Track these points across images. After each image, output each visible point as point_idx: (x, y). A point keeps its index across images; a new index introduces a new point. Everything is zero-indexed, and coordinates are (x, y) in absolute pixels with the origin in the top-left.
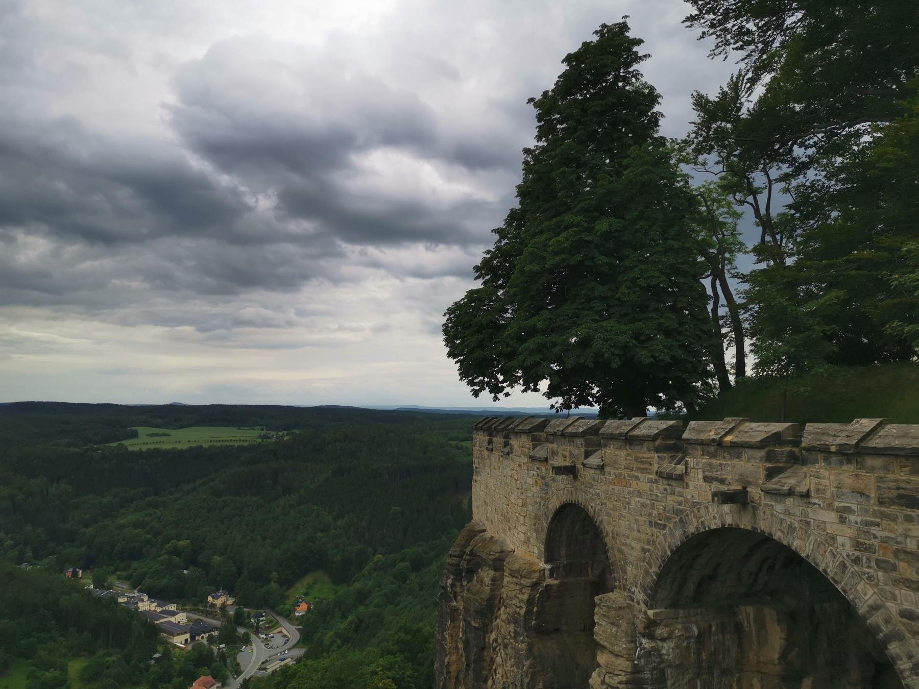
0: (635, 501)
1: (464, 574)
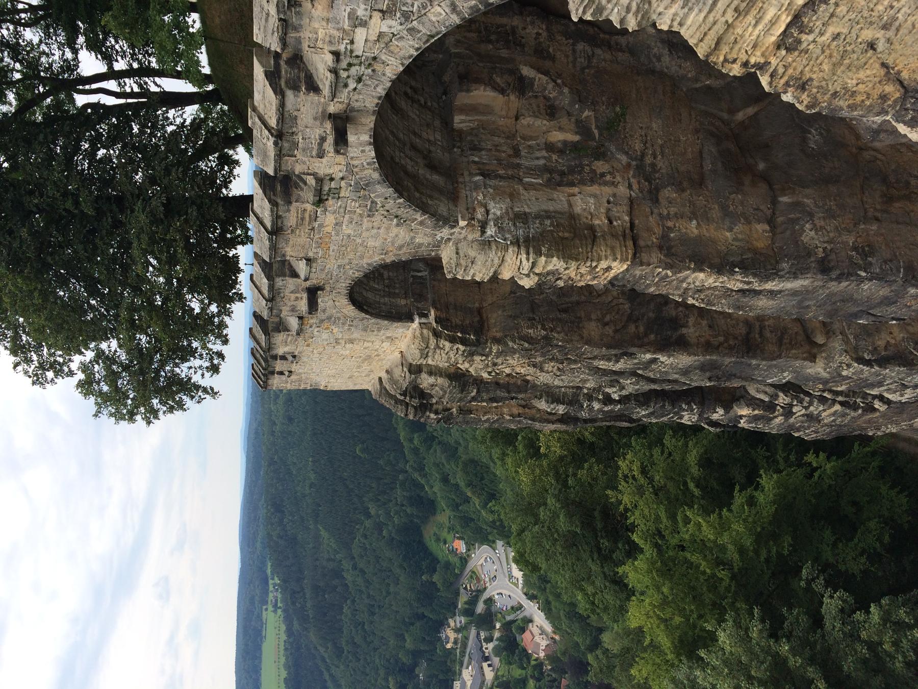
0: (347, 230)
1: (425, 402)
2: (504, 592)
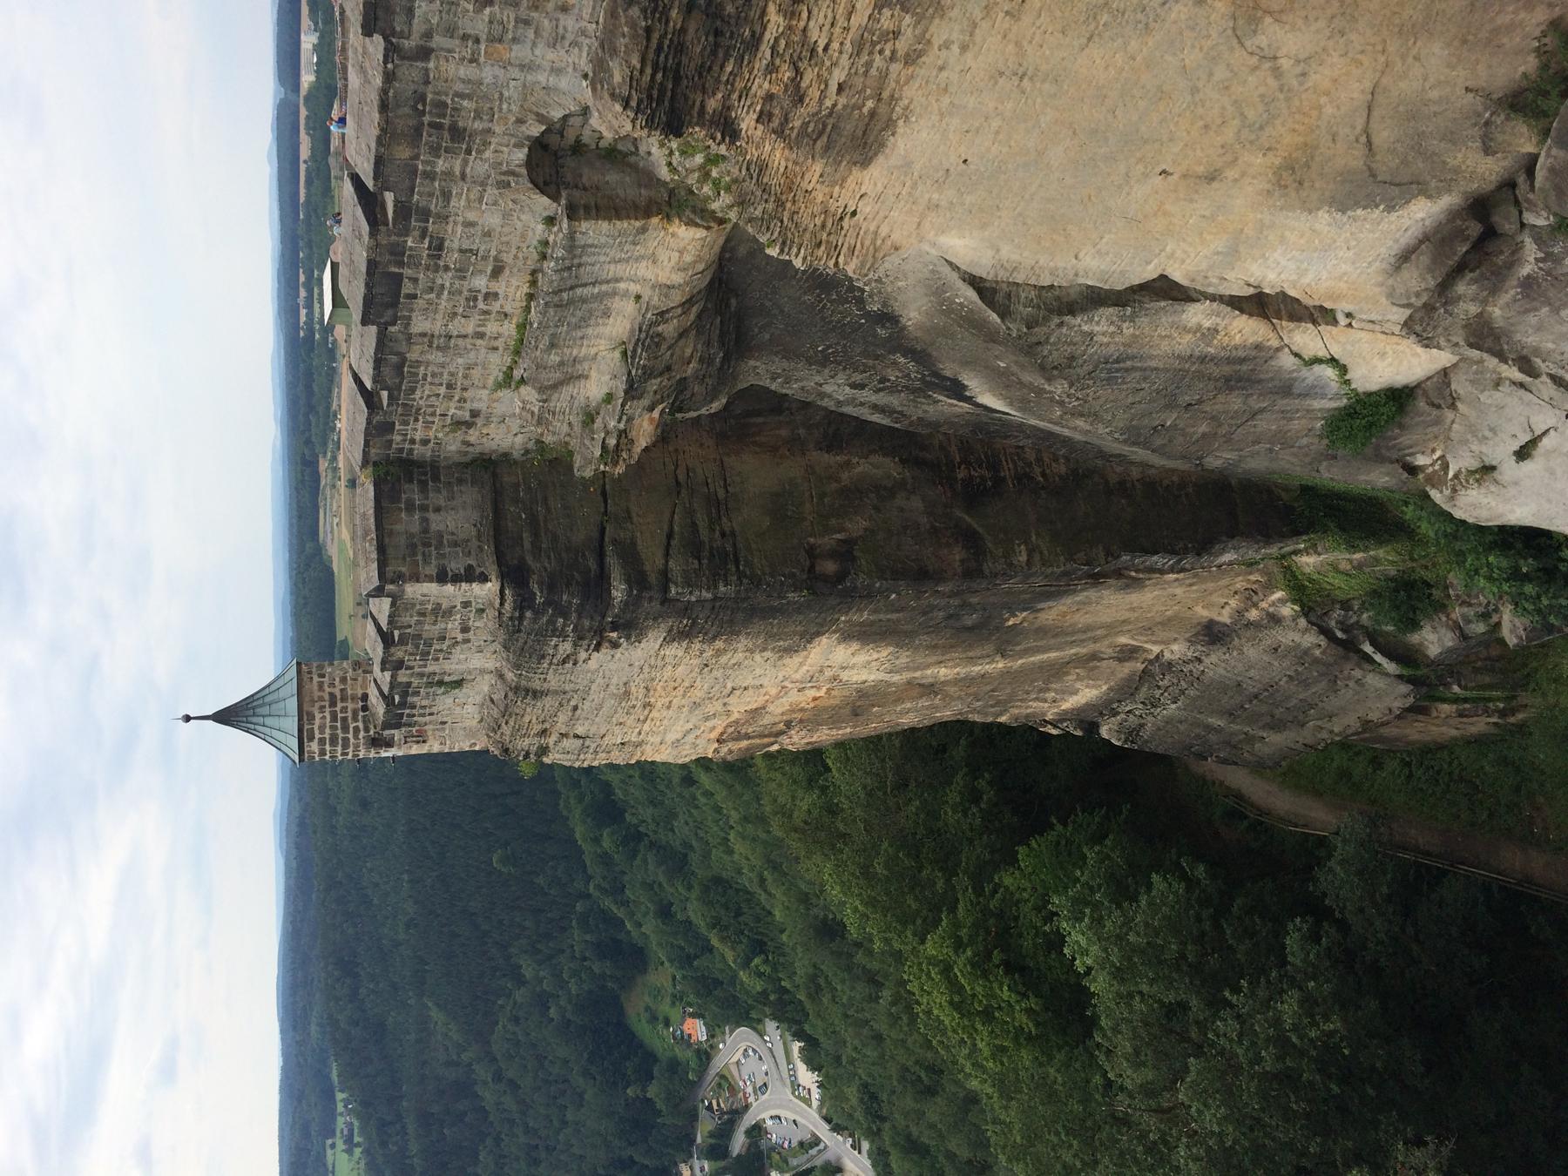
2: (782, 1113)
